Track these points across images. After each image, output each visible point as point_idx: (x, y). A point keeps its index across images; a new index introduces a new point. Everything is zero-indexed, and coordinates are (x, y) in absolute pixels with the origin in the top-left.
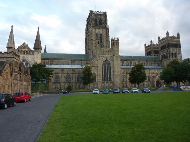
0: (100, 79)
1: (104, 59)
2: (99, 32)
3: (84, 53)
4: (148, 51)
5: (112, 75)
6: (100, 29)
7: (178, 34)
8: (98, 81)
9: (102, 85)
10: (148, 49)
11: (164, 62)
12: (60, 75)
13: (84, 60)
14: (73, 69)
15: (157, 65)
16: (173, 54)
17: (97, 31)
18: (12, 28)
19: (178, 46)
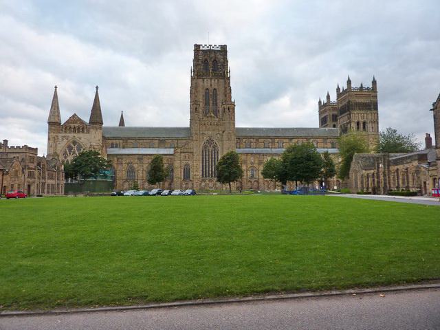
0: (197, 173)
2: (211, 85)
4: (322, 117)
7: (374, 82)
12: (136, 166)
15: (330, 145)
19: (372, 106)
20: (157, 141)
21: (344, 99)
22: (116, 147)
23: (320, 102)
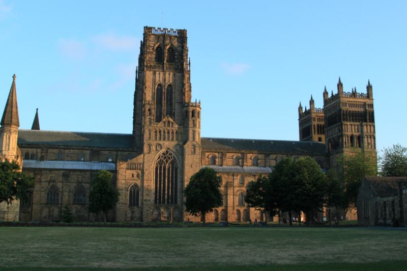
0: (148, 198)
3: (131, 132)
4: (305, 126)
5: (178, 190)
6: (167, 73)
7: (369, 88)
8: (142, 204)
11: (333, 158)
12: (60, 185)
13: (123, 151)
14: (91, 171)
16: (352, 137)
17: (159, 77)
19: (366, 116)
22: (32, 159)
23: (300, 108)
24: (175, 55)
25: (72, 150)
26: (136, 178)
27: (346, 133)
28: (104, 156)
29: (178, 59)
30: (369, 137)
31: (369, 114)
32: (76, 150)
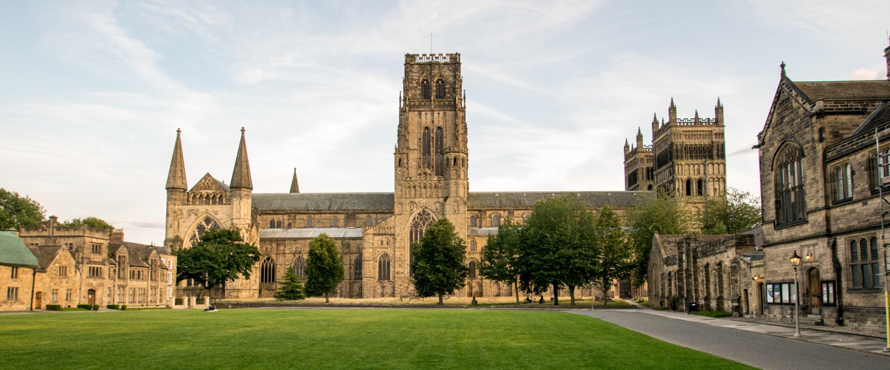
0: (401, 270)
1: (417, 211)
6: (436, 113)
8: (394, 278)
9: (407, 287)
10: (635, 162)
17: (426, 118)
18: (178, 135)
20: (342, 217)
21: (664, 140)
24: (445, 88)
25: (323, 215)
26: (386, 246)
27: (679, 177)
28: (362, 220)
29: (449, 93)
30: (716, 179)
31: (718, 147)
32: (328, 215)
